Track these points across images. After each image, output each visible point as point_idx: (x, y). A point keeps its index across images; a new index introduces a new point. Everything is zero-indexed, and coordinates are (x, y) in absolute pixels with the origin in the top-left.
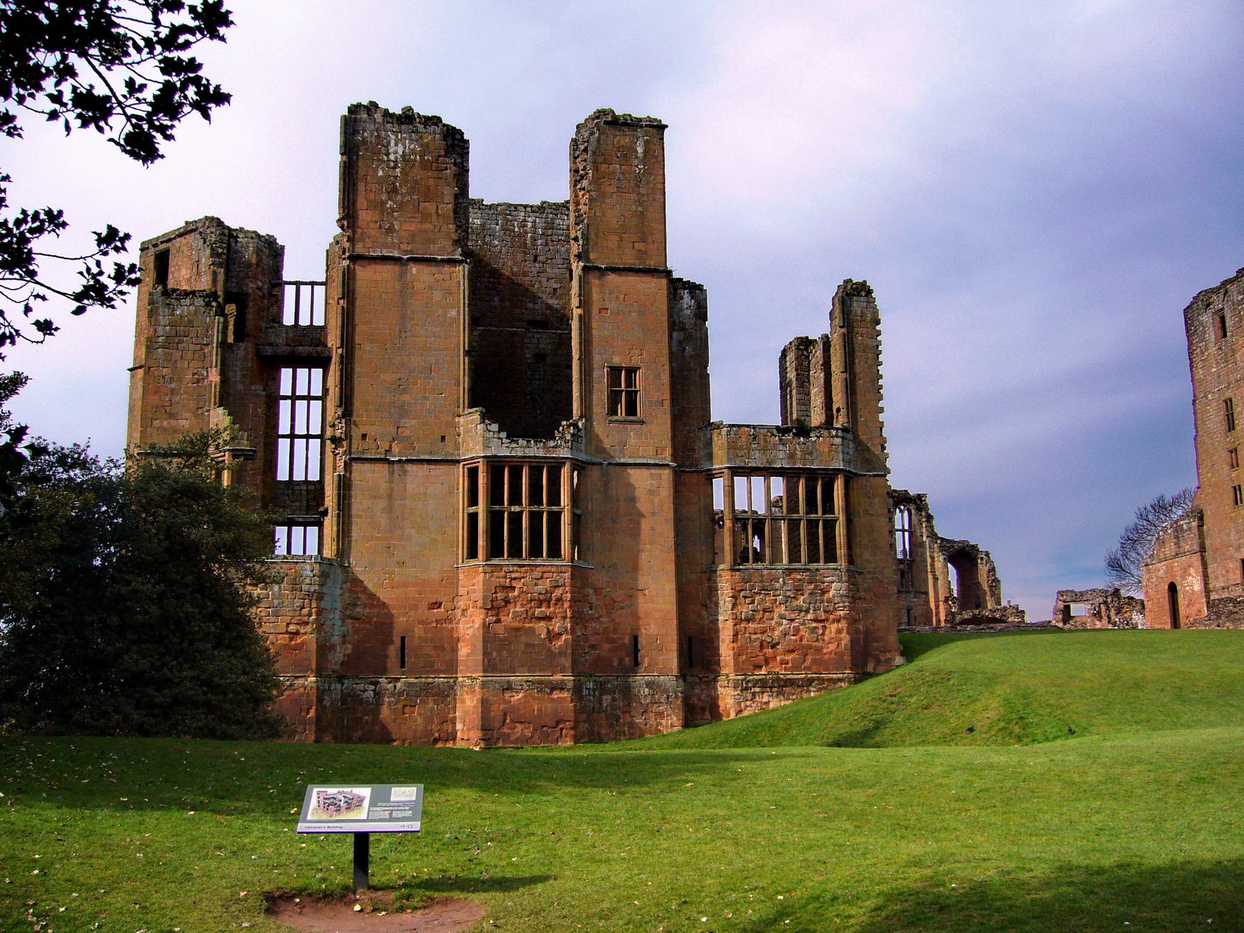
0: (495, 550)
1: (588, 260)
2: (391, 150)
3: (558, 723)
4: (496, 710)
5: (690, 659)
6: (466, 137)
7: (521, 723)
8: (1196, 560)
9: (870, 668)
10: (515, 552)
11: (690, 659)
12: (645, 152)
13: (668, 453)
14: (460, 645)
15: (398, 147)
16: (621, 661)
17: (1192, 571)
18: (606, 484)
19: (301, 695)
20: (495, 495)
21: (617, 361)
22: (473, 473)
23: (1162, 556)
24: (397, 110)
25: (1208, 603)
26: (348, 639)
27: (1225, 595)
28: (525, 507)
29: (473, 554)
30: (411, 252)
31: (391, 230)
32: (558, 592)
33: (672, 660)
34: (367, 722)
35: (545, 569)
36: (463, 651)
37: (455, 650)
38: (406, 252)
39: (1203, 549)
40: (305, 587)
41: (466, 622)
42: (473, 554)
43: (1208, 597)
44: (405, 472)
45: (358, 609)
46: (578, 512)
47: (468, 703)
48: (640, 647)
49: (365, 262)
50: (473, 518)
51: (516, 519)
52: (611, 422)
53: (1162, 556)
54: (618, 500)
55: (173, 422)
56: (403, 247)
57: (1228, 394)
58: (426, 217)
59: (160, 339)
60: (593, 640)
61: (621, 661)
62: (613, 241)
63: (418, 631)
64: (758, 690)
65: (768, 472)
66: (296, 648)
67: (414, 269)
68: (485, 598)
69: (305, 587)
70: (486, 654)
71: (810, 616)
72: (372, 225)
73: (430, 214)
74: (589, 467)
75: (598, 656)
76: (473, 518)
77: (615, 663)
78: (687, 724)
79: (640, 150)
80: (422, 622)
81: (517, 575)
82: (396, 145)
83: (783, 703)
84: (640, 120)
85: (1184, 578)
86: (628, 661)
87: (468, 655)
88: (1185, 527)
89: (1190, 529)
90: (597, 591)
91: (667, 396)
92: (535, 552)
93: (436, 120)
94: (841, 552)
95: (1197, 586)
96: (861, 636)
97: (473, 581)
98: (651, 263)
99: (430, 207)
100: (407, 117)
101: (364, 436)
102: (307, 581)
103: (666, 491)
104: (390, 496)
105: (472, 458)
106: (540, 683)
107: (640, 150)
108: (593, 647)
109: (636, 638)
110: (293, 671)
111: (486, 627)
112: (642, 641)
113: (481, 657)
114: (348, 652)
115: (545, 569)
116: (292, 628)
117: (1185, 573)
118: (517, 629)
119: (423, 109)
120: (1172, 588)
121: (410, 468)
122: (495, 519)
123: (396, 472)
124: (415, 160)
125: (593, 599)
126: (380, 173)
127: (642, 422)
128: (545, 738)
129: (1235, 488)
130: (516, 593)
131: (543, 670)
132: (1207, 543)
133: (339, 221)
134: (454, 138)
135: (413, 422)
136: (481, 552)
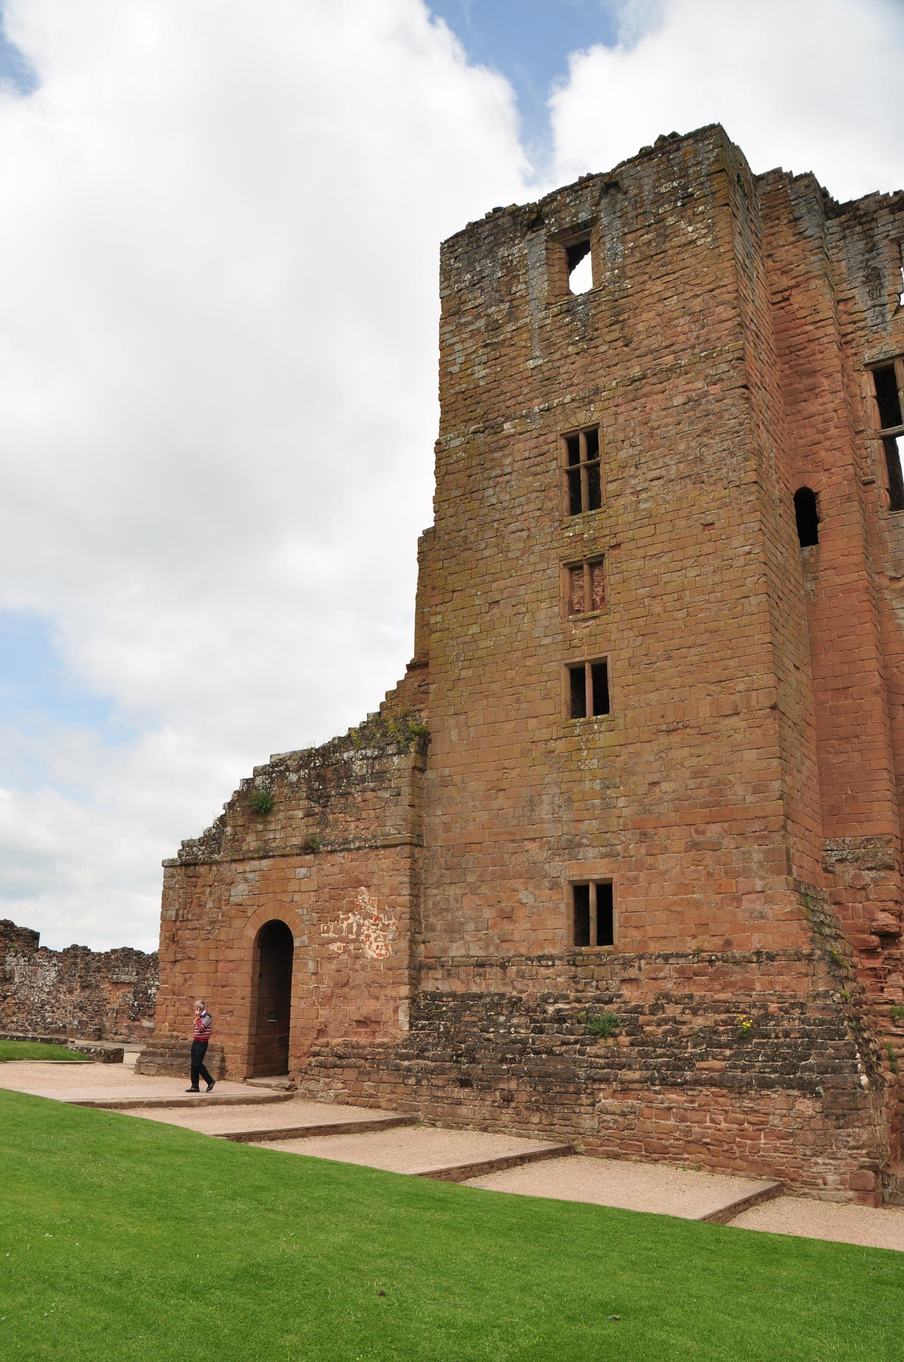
8: (389, 869)
17: (364, 896)
23: (251, 842)
25: (413, 1000)
27: (491, 984)
39: (416, 843)
43: (414, 982)
53: (251, 842)
57: (582, 418)
85: (326, 914)
88: (358, 768)
89: (380, 776)
95: (378, 945)
117: (335, 900)
120: (276, 943)
129: (576, 674)
132: (436, 818)
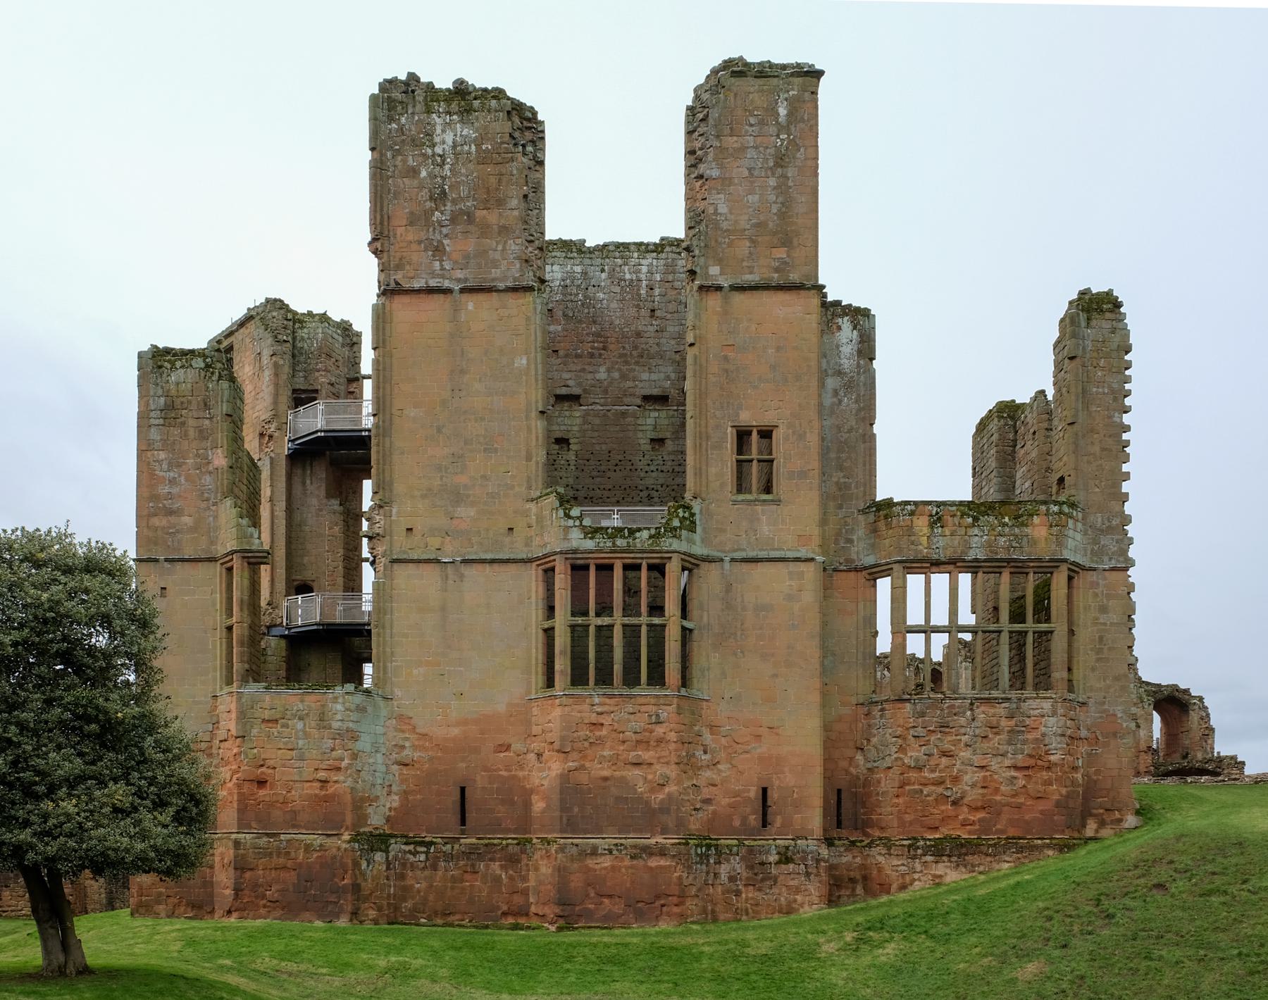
0: (578, 678)
1: (707, 275)
2: (437, 139)
3: (658, 897)
4: (576, 881)
5: (839, 814)
6: (540, 117)
7: (610, 896)
9: (1090, 831)
10: (605, 678)
11: (839, 814)
12: (790, 114)
13: (816, 541)
14: (534, 798)
15: (448, 134)
16: (744, 819)
18: (729, 588)
19: (334, 857)
20: (579, 609)
21: (746, 418)
22: (549, 572)
24: (444, 82)
26: (394, 788)
28: (618, 619)
29: (550, 683)
30: (466, 280)
31: (439, 250)
32: (660, 730)
33: (815, 820)
34: (419, 891)
35: (642, 700)
36: (538, 805)
37: (527, 805)
38: (459, 280)
40: (336, 725)
41: (541, 770)
42: (550, 683)
44: (462, 576)
45: (406, 752)
46: (687, 624)
47: (543, 870)
48: (769, 803)
49: (405, 299)
50: (549, 633)
51: (604, 633)
52: (735, 502)
54: (744, 609)
55: (173, 519)
56: (459, 274)
58: (485, 230)
59: (152, 414)
60: (706, 793)
61: (744, 819)
62: (743, 247)
63: (481, 780)
64: (929, 858)
65: (953, 564)
66: (326, 799)
67: (470, 303)
68: (563, 739)
69: (336, 725)
70: (564, 808)
71: (1007, 762)
72: (414, 247)
73: (488, 226)
74: (704, 565)
75: (714, 812)
76: (549, 633)
77: (737, 823)
78: (832, 901)
79: (782, 111)
80: (486, 769)
81: (606, 708)
82: (443, 131)
83: (966, 876)
84: (784, 67)
86: (754, 820)
87: (543, 811)
90: (713, 728)
91: (815, 464)
92: (631, 679)
93: (499, 94)
94: (1059, 674)
96: (1080, 790)
97: (554, 716)
98: (794, 277)
99: (492, 217)
100: (461, 91)
101: (409, 530)
102: (339, 717)
103: (809, 597)
104: (443, 609)
105: (545, 556)
106: (635, 847)
107: (782, 111)
108: (707, 801)
109: (765, 790)
110: (322, 829)
111: (565, 777)
112: (773, 795)
113: (557, 814)
114: (395, 805)
115: (642, 700)
116: (322, 775)
118: (606, 779)
119: (480, 79)
121: (471, 572)
122: (578, 633)
123: (451, 576)
124: (469, 153)
125: (707, 737)
126: (424, 174)
127: (777, 502)
128: (640, 916)
130: (604, 732)
131: (641, 831)
133: (370, 244)
134: (523, 118)
135: (472, 512)
136: (561, 680)
